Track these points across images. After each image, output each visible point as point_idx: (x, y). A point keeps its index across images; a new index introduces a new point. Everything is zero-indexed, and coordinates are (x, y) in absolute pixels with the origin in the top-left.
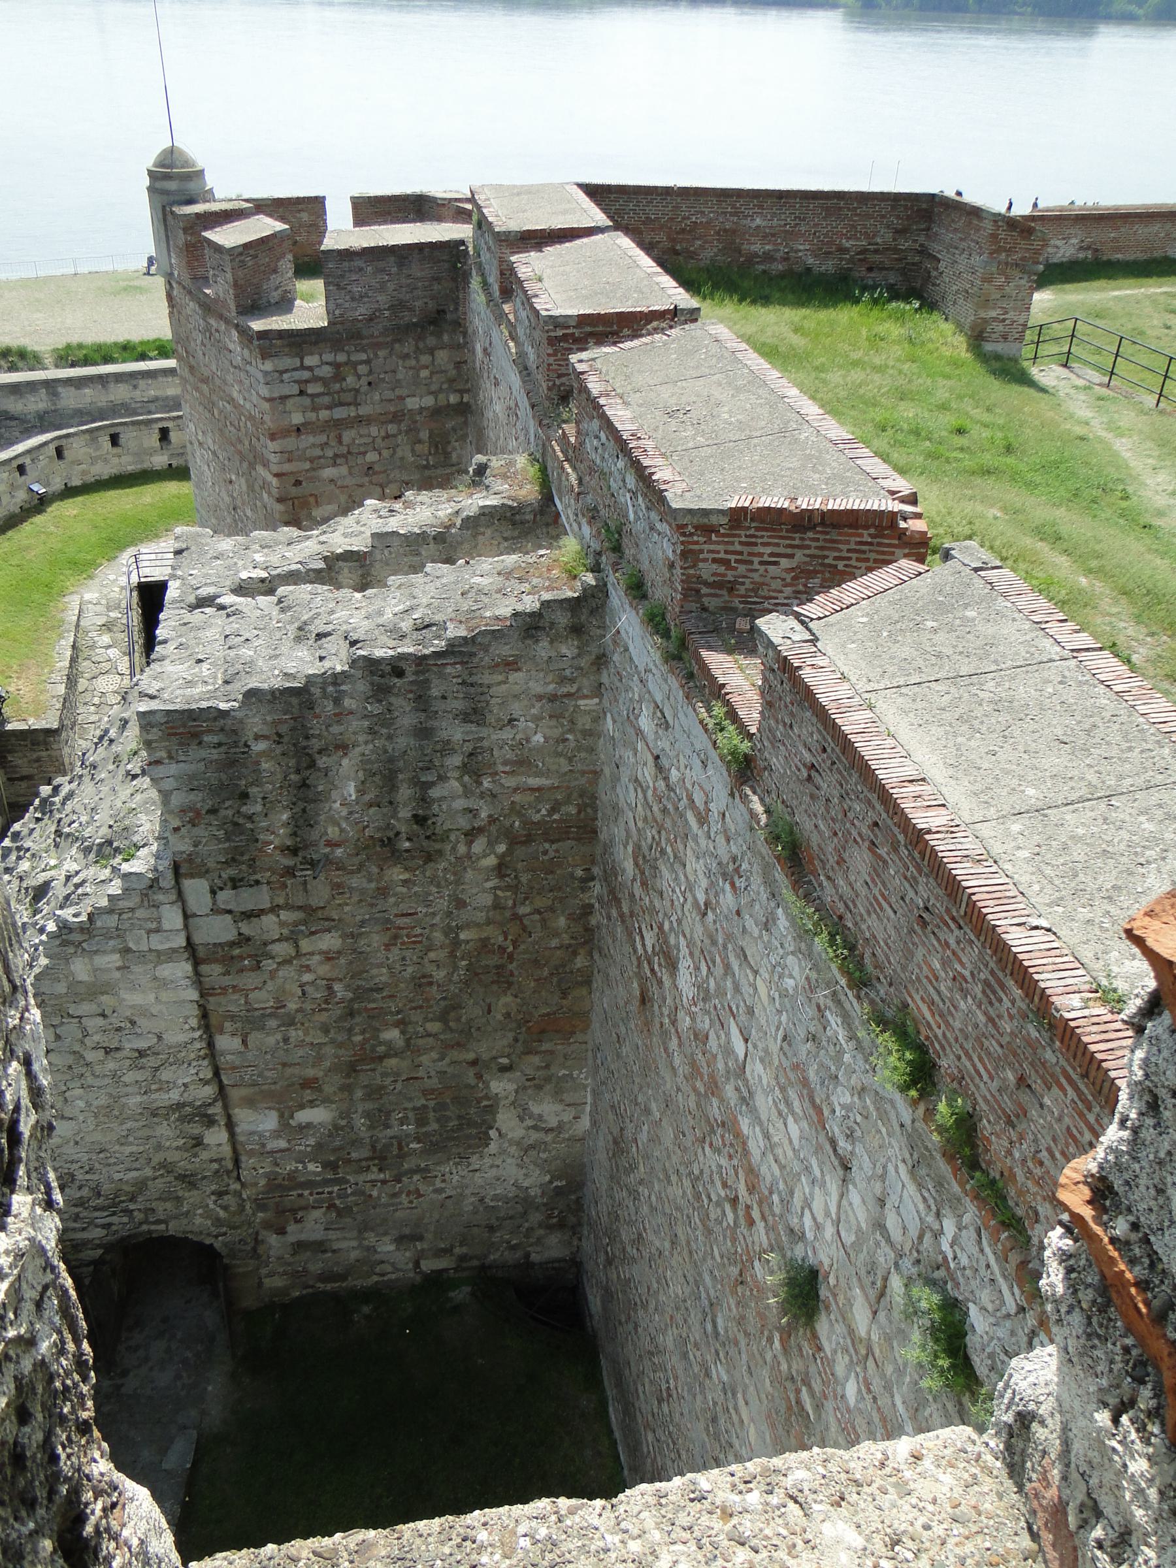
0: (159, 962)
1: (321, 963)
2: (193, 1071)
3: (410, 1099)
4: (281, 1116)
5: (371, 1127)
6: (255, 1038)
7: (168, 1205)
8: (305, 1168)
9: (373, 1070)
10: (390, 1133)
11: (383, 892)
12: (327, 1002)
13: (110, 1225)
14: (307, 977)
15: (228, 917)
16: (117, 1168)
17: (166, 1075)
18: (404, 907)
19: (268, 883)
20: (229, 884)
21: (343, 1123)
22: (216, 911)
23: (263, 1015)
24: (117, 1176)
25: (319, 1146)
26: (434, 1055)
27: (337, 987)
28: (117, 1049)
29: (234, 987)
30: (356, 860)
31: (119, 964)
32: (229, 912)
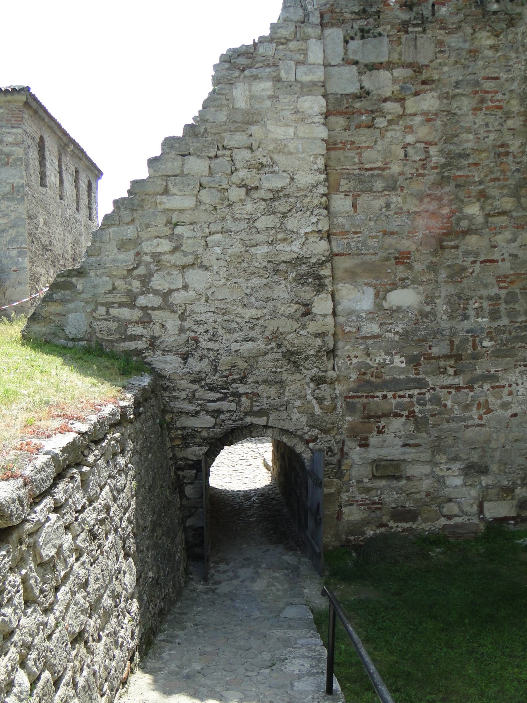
0: (302, 94)
1: (422, 123)
2: (314, 220)
3: (486, 286)
4: (377, 296)
5: (451, 317)
6: (363, 200)
7: (273, 391)
8: (392, 362)
9: (456, 247)
10: (466, 325)
11: (474, 53)
12: (424, 167)
13: (219, 412)
14: (410, 139)
15: (354, 68)
16: (236, 336)
17: (291, 224)
18: (491, 72)
19: (388, 36)
20: (359, 34)
21: (428, 308)
22: (347, 62)
23: (373, 176)
24: (235, 346)
25: (406, 335)
26: (508, 235)
27: (433, 151)
28: (256, 188)
29: (353, 143)
30: (456, 19)
31: (270, 93)
32: (356, 63)
